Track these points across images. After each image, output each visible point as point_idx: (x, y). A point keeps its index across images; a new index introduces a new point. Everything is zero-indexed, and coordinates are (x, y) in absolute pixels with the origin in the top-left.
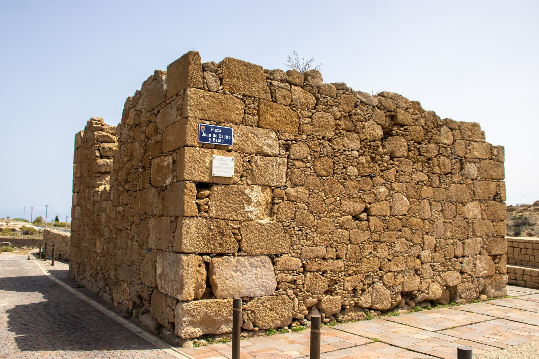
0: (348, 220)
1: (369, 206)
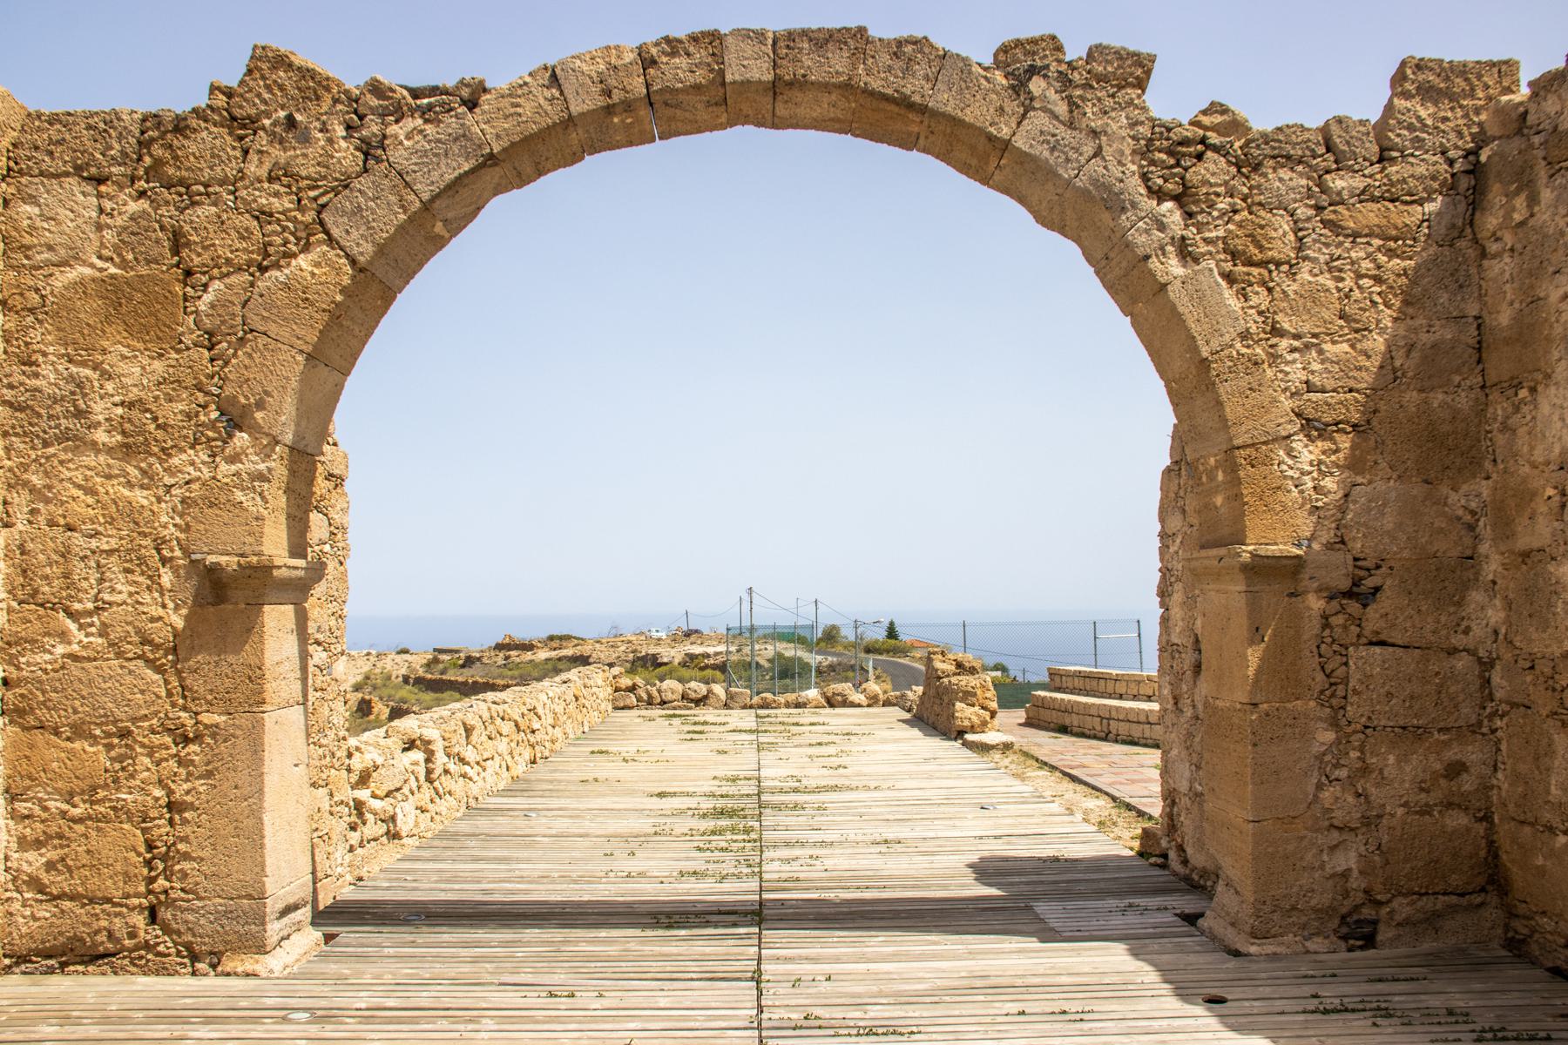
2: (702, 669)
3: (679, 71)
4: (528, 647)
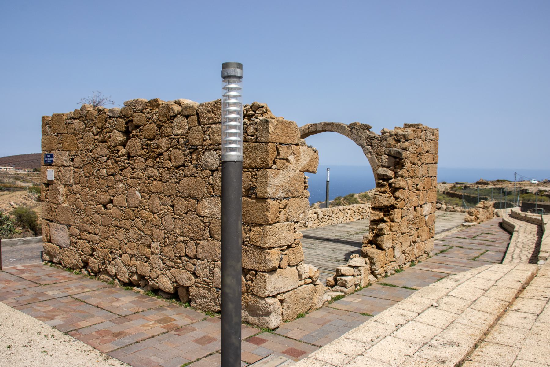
0: (100, 208)
1: (112, 198)
2: (542, 196)
3: (312, 129)
4: (487, 184)
